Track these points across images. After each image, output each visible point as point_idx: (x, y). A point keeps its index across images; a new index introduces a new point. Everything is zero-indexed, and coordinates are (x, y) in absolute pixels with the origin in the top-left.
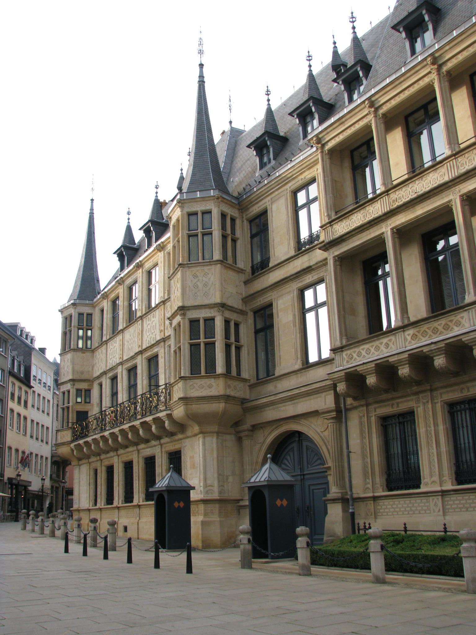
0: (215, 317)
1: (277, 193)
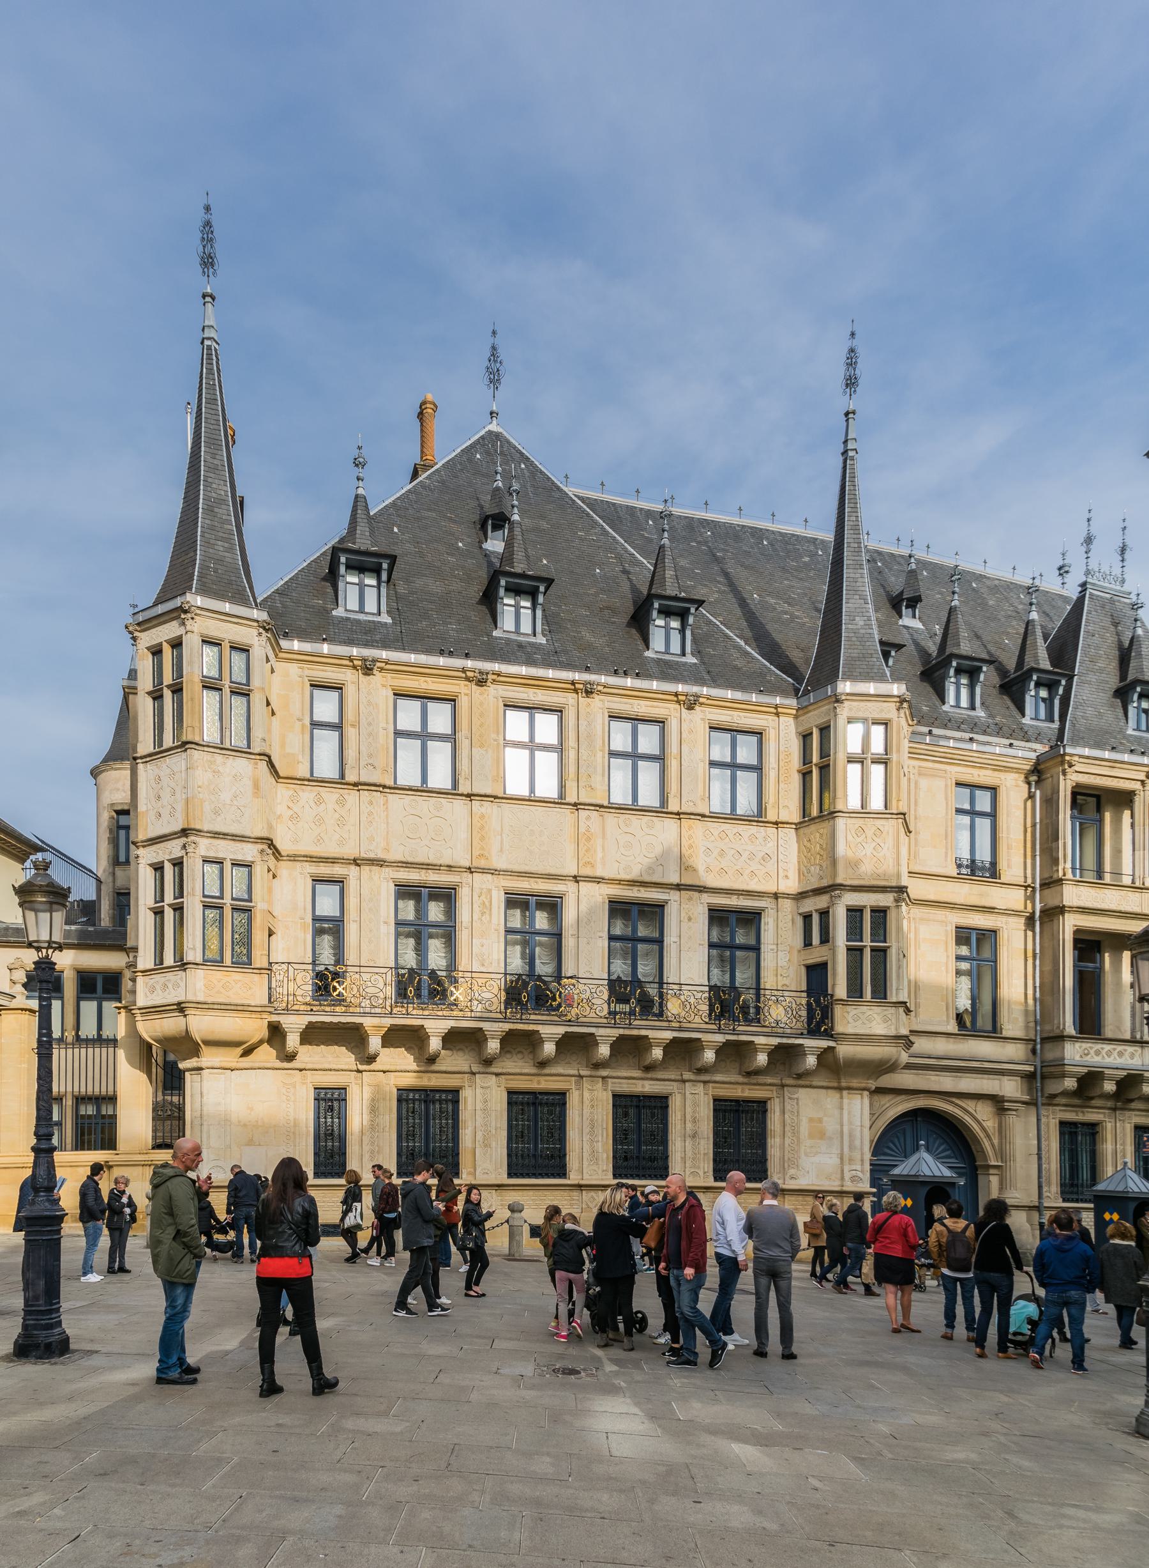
1: (930, 765)
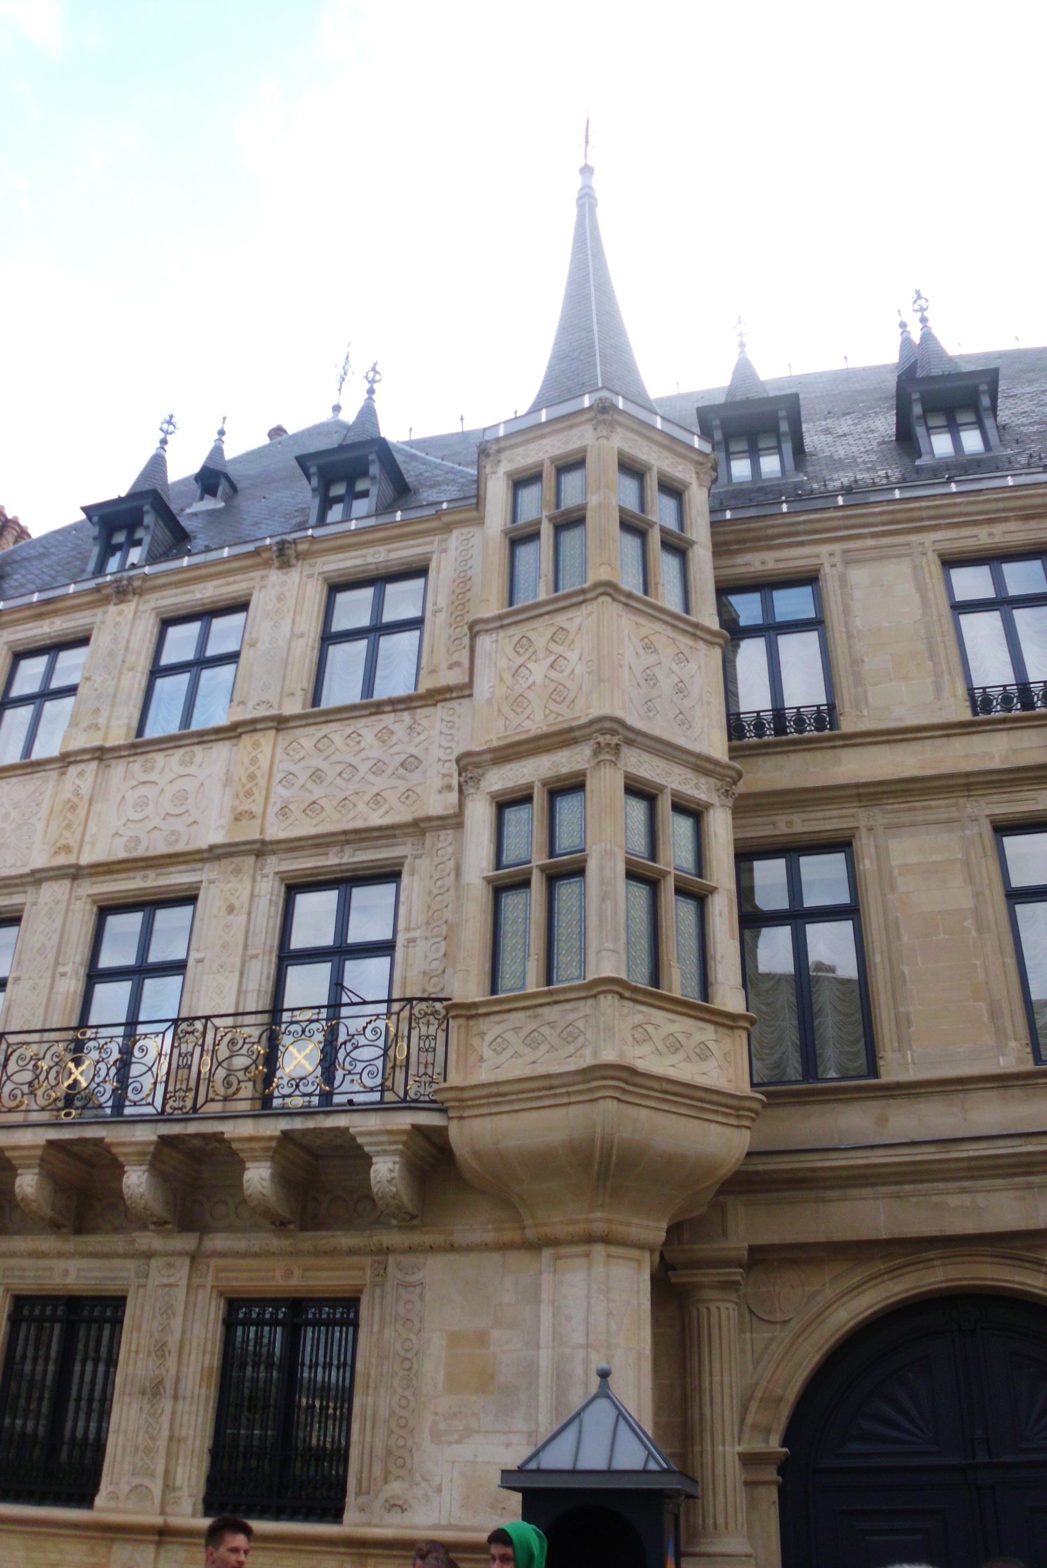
0: (708, 806)
1: (870, 542)
